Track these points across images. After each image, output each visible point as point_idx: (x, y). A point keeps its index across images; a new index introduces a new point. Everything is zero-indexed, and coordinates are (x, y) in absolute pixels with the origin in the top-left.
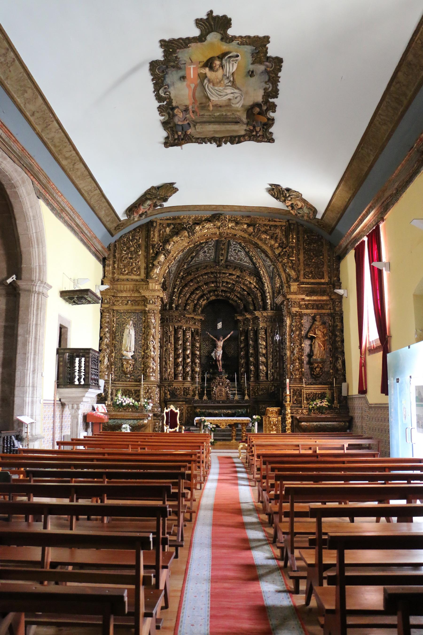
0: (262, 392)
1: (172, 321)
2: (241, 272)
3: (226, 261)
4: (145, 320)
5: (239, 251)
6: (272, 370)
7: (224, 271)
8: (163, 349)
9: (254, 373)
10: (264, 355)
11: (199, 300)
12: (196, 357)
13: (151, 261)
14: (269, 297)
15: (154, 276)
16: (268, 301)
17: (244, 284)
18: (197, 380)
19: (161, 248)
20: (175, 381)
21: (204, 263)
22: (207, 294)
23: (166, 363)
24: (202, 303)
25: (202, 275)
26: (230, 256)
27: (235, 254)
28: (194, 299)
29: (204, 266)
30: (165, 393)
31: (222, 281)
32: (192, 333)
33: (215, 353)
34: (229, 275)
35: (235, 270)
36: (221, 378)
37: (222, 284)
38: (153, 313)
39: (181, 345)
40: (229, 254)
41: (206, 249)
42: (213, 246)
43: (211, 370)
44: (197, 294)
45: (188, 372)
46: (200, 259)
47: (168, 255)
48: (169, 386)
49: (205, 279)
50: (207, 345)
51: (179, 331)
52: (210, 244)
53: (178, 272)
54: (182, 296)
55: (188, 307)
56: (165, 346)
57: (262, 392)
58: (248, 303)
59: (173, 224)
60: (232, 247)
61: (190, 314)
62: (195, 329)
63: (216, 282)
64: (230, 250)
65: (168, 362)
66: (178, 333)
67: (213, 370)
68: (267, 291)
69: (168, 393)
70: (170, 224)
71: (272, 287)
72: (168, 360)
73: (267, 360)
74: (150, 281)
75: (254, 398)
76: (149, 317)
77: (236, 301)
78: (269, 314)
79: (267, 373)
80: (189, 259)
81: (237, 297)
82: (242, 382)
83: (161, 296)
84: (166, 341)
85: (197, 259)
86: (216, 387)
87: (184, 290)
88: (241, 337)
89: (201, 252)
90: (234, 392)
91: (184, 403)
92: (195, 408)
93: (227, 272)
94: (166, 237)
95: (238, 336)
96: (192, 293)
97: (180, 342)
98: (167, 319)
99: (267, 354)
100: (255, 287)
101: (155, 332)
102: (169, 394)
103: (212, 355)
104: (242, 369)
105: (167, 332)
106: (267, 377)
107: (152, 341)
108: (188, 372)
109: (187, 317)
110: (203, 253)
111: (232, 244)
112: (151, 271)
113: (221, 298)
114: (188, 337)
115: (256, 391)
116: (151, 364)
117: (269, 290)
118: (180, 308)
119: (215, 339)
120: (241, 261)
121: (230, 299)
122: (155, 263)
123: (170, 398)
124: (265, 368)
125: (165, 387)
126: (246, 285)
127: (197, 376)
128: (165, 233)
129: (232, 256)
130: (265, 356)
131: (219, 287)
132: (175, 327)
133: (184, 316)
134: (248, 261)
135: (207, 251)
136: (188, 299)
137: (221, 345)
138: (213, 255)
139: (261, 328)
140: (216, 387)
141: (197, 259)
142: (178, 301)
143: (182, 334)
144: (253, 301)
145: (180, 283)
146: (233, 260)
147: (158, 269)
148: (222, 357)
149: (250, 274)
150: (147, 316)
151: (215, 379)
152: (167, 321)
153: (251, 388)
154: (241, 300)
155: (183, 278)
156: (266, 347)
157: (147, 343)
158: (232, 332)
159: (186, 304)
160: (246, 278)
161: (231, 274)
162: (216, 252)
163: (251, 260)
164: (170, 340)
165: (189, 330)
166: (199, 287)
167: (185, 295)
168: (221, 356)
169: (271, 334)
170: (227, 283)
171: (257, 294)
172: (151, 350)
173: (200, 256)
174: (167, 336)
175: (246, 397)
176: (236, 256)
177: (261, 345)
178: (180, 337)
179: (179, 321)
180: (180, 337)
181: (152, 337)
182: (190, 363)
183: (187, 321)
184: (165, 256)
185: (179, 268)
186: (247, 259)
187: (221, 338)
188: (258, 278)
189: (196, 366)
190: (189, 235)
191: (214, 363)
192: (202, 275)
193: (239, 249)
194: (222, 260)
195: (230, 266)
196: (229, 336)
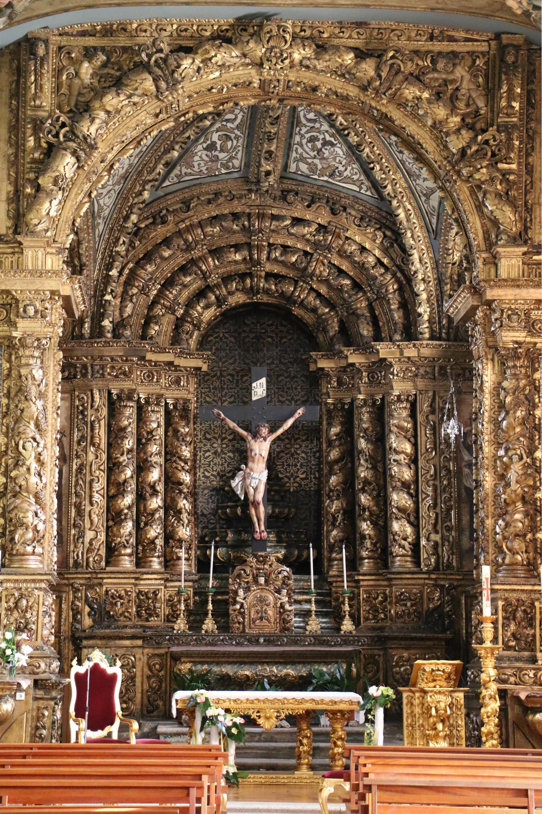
0: (400, 609)
1: (103, 375)
2: (333, 212)
3: (282, 177)
4: (10, 370)
5: (326, 143)
6: (433, 537)
7: (275, 212)
8: (70, 467)
9: (374, 545)
10: (405, 486)
11: (190, 304)
12: (181, 492)
13: (32, 176)
14: (424, 296)
15: (40, 227)
17: (342, 253)
18: (183, 566)
19: (63, 131)
20: (108, 569)
21: (209, 184)
23: (80, 512)
24: (201, 315)
26: (296, 160)
27: (312, 154)
28: (175, 301)
30: (76, 612)
31: (270, 245)
32: (168, 413)
33: (244, 479)
34: (293, 225)
35: (314, 207)
36: (264, 562)
37: (269, 253)
38: (38, 347)
39: (130, 451)
40: (294, 155)
41: (215, 137)
42: (237, 127)
43: (230, 536)
44: (185, 286)
45: (153, 542)
46: (196, 169)
47: (89, 156)
48: (90, 587)
49: (213, 236)
50: (215, 453)
51: (126, 406)
53: (120, 212)
54: (135, 291)
55: (154, 329)
56: (78, 457)
57: (400, 609)
58: (354, 314)
59: (103, 49)
60: (304, 130)
61: (163, 351)
62: (177, 399)
63: (249, 246)
64: (297, 138)
65: (88, 508)
66: (121, 413)
67: (237, 532)
68: (420, 277)
69: (87, 609)
70: (95, 48)
72: (87, 502)
73: (417, 503)
74: (26, 241)
75: (373, 629)
76: (23, 361)
77: (314, 310)
79: (416, 546)
80: (160, 169)
81: (319, 295)
82: (331, 573)
83: (66, 291)
84: (83, 438)
85: (184, 170)
86: (247, 590)
87: (142, 273)
88: (330, 425)
89: (200, 147)
90: (306, 607)
91: (139, 642)
92: (176, 658)
93: (284, 212)
94: (80, 94)
95: (321, 423)
96: (168, 283)
97: (129, 443)
98: (85, 367)
99: (416, 482)
101: (45, 409)
102: (89, 614)
103: (234, 484)
104: (334, 533)
105: (85, 409)
106: (417, 562)
107: (34, 439)
108: (153, 542)
109: (150, 361)
111: (303, 121)
112: (30, 207)
113: (265, 299)
114: (154, 425)
115: (381, 603)
116: (30, 515)
117: (425, 274)
118: (128, 333)
119: (244, 433)
120: (331, 176)
121: (295, 302)
122: (45, 181)
123: (91, 627)
124: (409, 530)
125: (77, 590)
126: (349, 257)
127: (182, 554)
128: (77, 81)
129: (302, 159)
130: (409, 488)
131: (259, 263)
132: (110, 394)
133: (143, 358)
135: (219, 143)
136: (155, 303)
137: (265, 454)
138: (239, 155)
139: (399, 397)
140: (247, 590)
141: (184, 170)
142: (122, 309)
143: (135, 416)
144: (371, 308)
145: (127, 250)
147: (55, 202)
148: (268, 491)
149: (362, 219)
150: (18, 357)
151: (244, 562)
152: (84, 375)
153: (363, 596)
154: (333, 307)
155: (137, 232)
156: (414, 460)
157: (17, 445)
158: (300, 411)
159: (149, 320)
160: (348, 234)
161: (297, 221)
162: (248, 147)
163: (368, 172)
164: (92, 437)
165: (158, 404)
166: (193, 262)
167: (144, 291)
168: (262, 489)
169: (431, 417)
170: (285, 248)
171: (386, 286)
172: (28, 469)
173: (196, 158)
174: (86, 423)
175: (347, 625)
177: (397, 452)
178: (125, 428)
179: (124, 373)
180: (125, 428)
181: (32, 426)
182: (162, 512)
183: (150, 376)
184: (78, 159)
185: (126, 199)
187: (264, 431)
188: (388, 233)
189: (179, 520)
190: (157, 88)
191: (239, 511)
193: (328, 138)
194: (268, 173)
195: (297, 194)
196: (290, 422)
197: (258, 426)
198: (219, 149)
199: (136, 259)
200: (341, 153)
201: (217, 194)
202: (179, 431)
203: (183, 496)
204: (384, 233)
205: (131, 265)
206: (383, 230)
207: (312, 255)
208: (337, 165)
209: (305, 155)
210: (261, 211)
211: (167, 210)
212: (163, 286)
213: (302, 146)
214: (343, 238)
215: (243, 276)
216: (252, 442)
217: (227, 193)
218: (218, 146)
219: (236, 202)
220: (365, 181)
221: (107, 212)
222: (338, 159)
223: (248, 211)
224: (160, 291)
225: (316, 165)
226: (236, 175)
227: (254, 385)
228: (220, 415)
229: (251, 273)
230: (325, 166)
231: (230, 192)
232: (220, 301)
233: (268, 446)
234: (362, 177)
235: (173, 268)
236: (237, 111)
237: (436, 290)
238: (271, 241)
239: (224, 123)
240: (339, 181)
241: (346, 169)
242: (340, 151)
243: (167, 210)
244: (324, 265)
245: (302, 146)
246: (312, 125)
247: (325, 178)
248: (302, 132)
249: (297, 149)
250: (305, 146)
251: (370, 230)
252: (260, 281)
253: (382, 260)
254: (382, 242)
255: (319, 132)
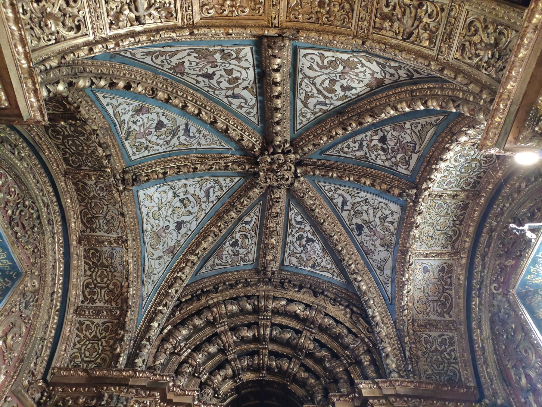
2: (315, 296)
5: (309, 240)
16: (389, 361)
22: (234, 360)
25: (224, 302)
27: (300, 249)
29: (230, 280)
34: (287, 304)
37: (271, 331)
40: (288, 251)
41: (238, 236)
52: (246, 223)
60: (294, 231)
64: (290, 238)
71: (395, 322)
78: (401, 390)
81: (307, 369)
100: (350, 331)
110: (231, 245)
111: (294, 223)
120: (313, 266)
134: (329, 267)
135: (240, 240)
144: (347, 372)
146: (297, 264)
161: (290, 301)
162: (259, 244)
163: (338, 260)
176: (303, 255)
186: (327, 262)
188: (355, 309)
192: (224, 302)
198: (240, 245)
199: (175, 324)
200: (319, 248)
201: (237, 284)
204: (352, 310)
205: (169, 327)
206: (351, 307)
207: (301, 333)
208: (316, 258)
209: (295, 251)
210: (267, 293)
211: (202, 291)
212: (192, 351)
213: (293, 244)
214: (324, 313)
215: (252, 354)
217: (244, 280)
218: (239, 243)
219: (249, 288)
220: (335, 270)
221: (156, 277)
222: (317, 252)
223: (257, 294)
224: (190, 354)
225: (302, 258)
226: (250, 267)
229: (257, 323)
230: (309, 258)
231: (246, 280)
232: (234, 376)
234: (334, 267)
235: (202, 338)
236: (252, 215)
237: (398, 344)
238: (273, 321)
239: (244, 225)
240: (318, 270)
241: (322, 261)
242: (318, 246)
243: (202, 291)
244: (310, 339)
245: (293, 244)
246: (299, 226)
247: (309, 269)
248: (293, 233)
249: (290, 247)
250: (295, 244)
251: (341, 307)
252: (265, 357)
253: (353, 330)
254: (351, 317)
255: (304, 232)
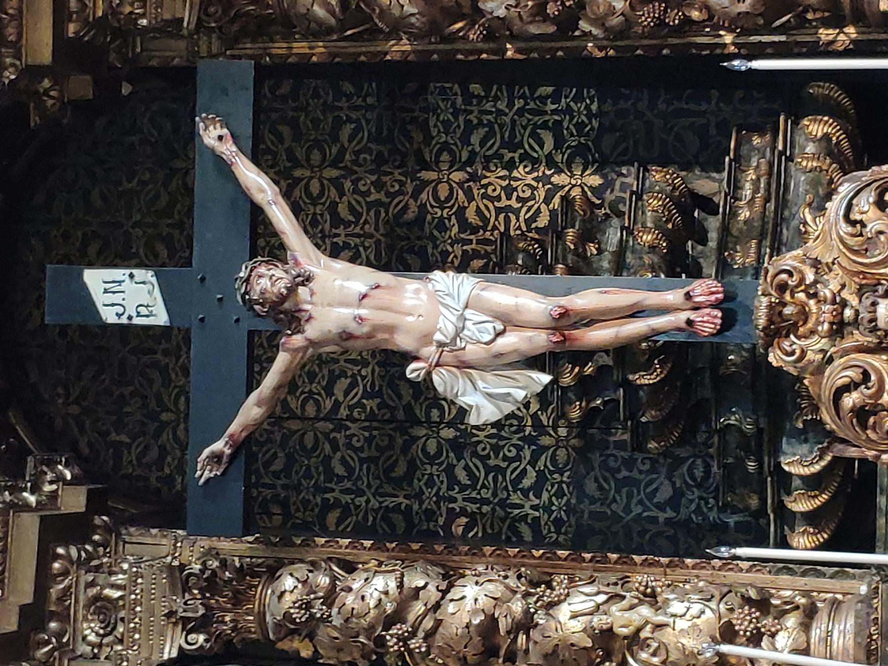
33: (463, 365)
119: (282, 360)
197: (249, 304)
202: (287, 616)
203: (540, 618)
216: (312, 331)
227: (109, 316)
228: (217, 458)
233: (339, 265)
